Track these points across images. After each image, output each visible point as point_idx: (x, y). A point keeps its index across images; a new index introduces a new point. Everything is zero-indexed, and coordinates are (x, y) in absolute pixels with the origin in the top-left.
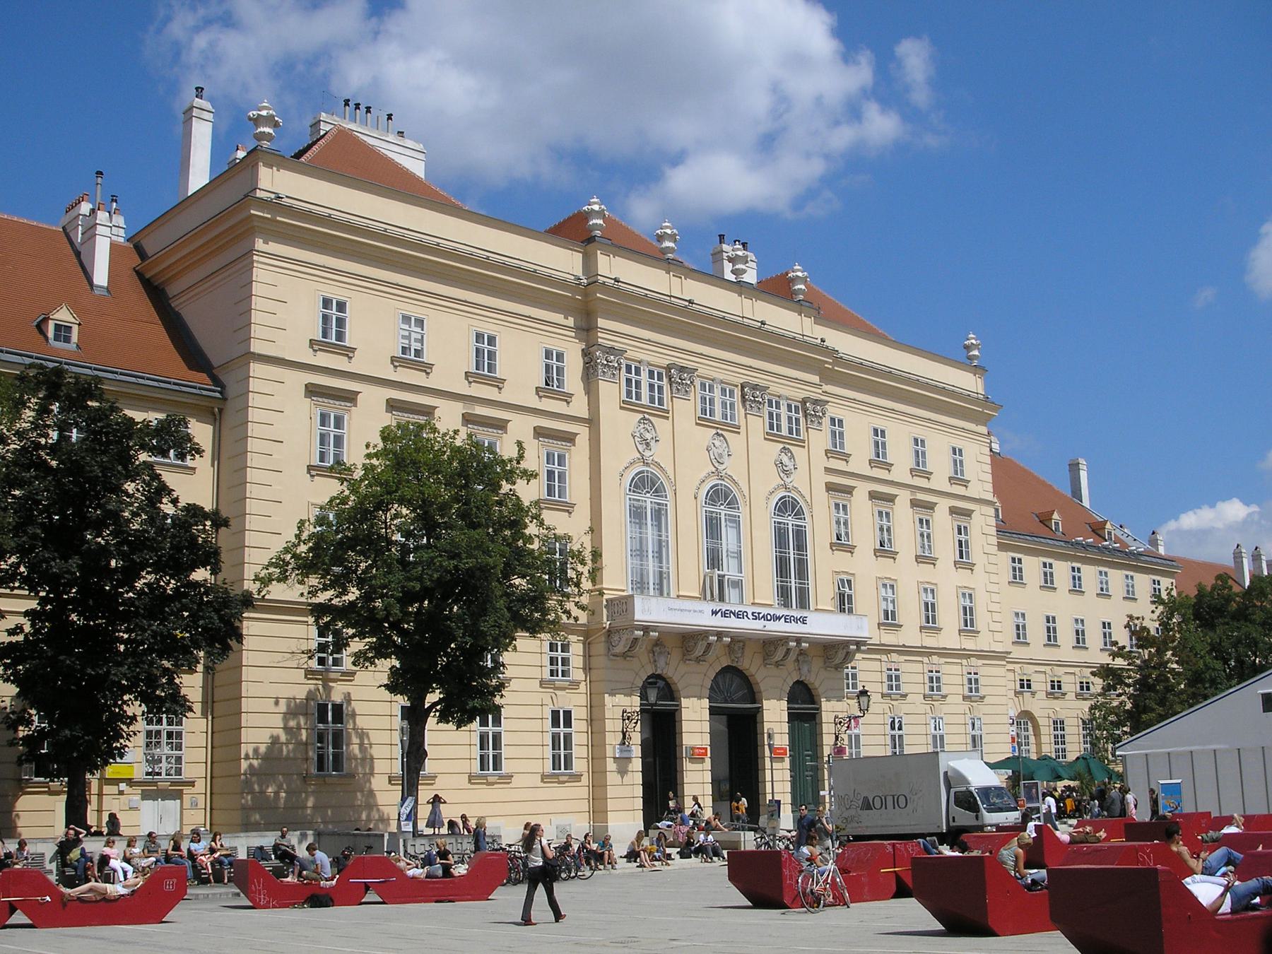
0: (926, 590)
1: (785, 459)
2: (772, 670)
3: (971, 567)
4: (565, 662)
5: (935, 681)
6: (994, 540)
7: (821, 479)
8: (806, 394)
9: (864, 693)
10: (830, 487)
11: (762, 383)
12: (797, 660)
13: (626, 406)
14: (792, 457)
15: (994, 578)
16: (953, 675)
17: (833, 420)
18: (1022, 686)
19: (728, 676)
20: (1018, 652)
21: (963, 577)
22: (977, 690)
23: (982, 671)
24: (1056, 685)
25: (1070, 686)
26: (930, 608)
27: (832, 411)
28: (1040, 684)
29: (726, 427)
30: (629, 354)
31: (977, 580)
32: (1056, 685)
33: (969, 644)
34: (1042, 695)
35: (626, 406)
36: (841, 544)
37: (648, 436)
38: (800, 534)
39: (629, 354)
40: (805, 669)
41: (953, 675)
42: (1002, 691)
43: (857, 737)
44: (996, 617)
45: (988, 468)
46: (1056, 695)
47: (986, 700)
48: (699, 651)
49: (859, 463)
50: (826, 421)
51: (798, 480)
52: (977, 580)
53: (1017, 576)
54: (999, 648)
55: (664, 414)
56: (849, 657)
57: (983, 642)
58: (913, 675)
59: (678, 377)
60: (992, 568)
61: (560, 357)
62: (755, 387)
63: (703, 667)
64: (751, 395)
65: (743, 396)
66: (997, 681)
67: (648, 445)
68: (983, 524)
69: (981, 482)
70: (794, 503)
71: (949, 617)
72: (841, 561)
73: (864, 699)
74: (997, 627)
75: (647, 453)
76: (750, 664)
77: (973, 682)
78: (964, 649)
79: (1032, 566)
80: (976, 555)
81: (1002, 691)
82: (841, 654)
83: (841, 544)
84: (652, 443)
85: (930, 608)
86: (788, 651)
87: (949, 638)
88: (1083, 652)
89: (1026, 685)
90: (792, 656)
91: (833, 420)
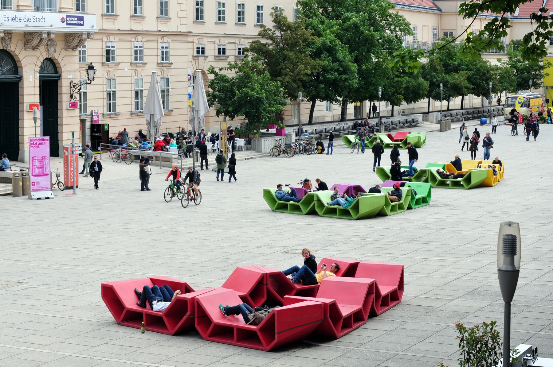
2: (30, 52)
12: (47, 45)
18: (198, 52)
23: (171, 46)
24: (222, 51)
28: (211, 51)
32: (222, 51)
33: (163, 27)
40: (52, 50)
42: (184, 59)
44: (183, 7)
46: (221, 58)
54: (183, 29)
57: (173, 26)
74: (182, 14)
77: (165, 55)
78: (160, 31)
81: (184, 59)
89: (201, 51)
90: (44, 42)
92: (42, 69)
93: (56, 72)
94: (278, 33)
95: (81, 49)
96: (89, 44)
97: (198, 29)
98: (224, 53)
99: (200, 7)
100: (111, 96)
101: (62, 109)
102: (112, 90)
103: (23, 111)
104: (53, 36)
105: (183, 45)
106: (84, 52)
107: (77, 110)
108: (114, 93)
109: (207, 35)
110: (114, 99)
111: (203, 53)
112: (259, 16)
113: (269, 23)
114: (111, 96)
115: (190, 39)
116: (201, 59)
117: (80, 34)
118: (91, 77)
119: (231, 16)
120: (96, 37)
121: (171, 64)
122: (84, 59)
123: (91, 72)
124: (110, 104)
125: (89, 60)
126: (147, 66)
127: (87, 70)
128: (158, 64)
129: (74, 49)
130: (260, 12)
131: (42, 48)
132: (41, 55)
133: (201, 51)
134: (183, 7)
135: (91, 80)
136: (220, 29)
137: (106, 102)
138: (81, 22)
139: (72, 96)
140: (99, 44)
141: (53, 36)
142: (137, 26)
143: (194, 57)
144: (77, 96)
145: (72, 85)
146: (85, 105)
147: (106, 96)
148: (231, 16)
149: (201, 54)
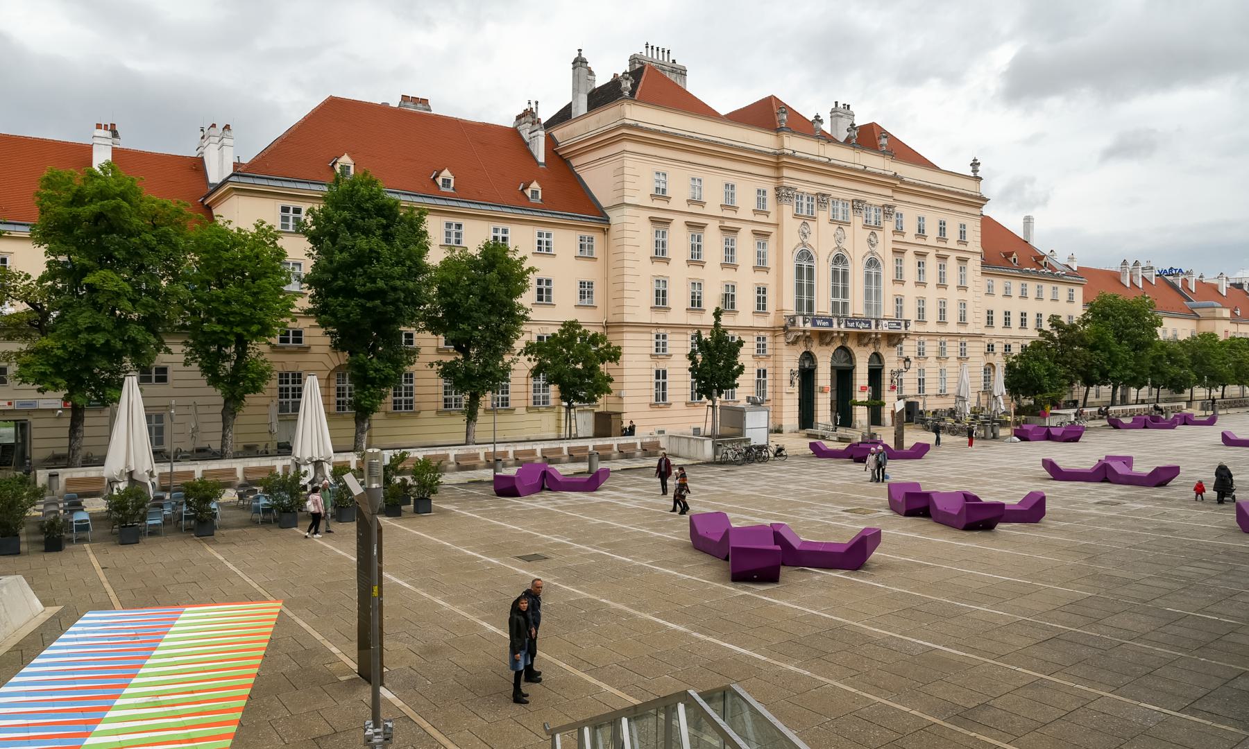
2: (862, 348)
3: (965, 288)
4: (764, 346)
5: (942, 350)
6: (980, 274)
7: (890, 246)
8: (882, 203)
9: (907, 360)
11: (863, 199)
13: (796, 216)
14: (876, 237)
15: (978, 294)
17: (897, 214)
18: (989, 350)
19: (839, 350)
20: (989, 332)
21: (961, 295)
22: (965, 354)
24: (1008, 347)
26: (942, 312)
27: (897, 210)
28: (999, 348)
29: (842, 224)
30: (799, 189)
31: (968, 296)
32: (1008, 347)
33: (963, 330)
34: (999, 355)
35: (796, 216)
36: (898, 280)
37: (806, 231)
38: (878, 276)
39: (799, 189)
41: (952, 348)
42: (978, 354)
43: (901, 379)
44: (978, 315)
45: (979, 234)
47: (969, 360)
48: (828, 339)
50: (894, 216)
51: (879, 249)
52: (968, 296)
53: (990, 293)
54: (978, 332)
55: (814, 219)
56: (900, 341)
58: (931, 348)
59: (822, 199)
60: (976, 289)
61: (764, 192)
62: (859, 201)
63: (829, 347)
64: (857, 206)
65: (853, 206)
66: (976, 350)
67: (806, 236)
68: (975, 263)
69: (974, 241)
70: (876, 261)
71: (952, 316)
72: (899, 290)
73: (907, 363)
74: (978, 320)
75: (805, 240)
76: (851, 345)
79: (999, 284)
80: (969, 283)
81: (978, 354)
82: (896, 341)
83: (898, 280)
84: (808, 235)
85: (942, 312)
86: (870, 339)
87: (952, 327)
88: (1025, 330)
89: (991, 348)
90: (873, 341)
91: (897, 214)
92: (870, 360)
93: (880, 363)
95: (899, 346)
96: (905, 342)
97: (989, 332)
99: (990, 315)
100: (921, 381)
102: (922, 377)
104: (879, 336)
106: (901, 349)
107: (896, 391)
108: (923, 379)
109: (996, 337)
110: (923, 384)
111: (992, 350)
112: (1039, 321)
113: (1046, 326)
114: (921, 381)
115: (983, 339)
117: (900, 334)
118: (907, 366)
119: (1015, 321)
120: (911, 337)
121: (968, 358)
122: (901, 353)
125: (905, 355)
126: (949, 360)
127: (905, 362)
128: (958, 358)
129: (894, 345)
130: (1024, 317)
131: (871, 345)
132: (870, 350)
133: (991, 348)
134: (978, 315)
135: (907, 369)
136: (1007, 332)
137: (917, 386)
140: (912, 343)
141: (879, 336)
142: (942, 329)
143: (985, 353)
144: (896, 380)
145: (892, 373)
146: (901, 388)
147: (917, 381)
148: (1015, 321)
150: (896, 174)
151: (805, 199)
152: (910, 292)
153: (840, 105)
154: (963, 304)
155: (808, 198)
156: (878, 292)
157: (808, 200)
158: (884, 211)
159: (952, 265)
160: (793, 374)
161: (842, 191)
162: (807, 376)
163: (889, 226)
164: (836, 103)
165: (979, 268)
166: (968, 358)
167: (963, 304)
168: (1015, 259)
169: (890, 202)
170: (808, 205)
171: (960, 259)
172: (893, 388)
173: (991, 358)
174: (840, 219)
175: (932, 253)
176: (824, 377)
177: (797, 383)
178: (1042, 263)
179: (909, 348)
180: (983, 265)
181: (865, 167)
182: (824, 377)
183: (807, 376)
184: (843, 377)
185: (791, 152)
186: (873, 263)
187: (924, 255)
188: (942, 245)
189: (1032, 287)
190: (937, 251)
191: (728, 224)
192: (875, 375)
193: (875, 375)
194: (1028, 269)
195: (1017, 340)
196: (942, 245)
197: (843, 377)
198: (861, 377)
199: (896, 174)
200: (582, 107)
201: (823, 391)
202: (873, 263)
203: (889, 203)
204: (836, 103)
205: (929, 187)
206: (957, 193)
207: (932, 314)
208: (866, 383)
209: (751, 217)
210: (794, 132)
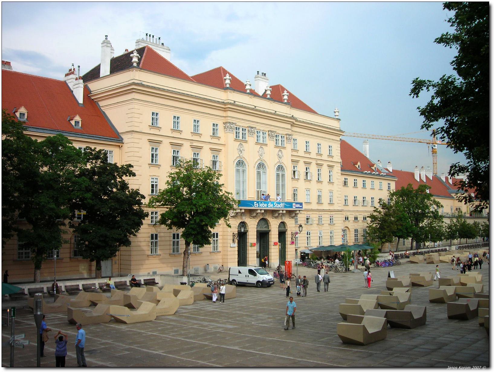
0: (319, 191)
1: (280, 154)
5: (320, 219)
7: (290, 158)
8: (287, 133)
9: (301, 226)
10: (292, 161)
13: (236, 140)
16: (326, 218)
17: (294, 139)
18: (346, 219)
20: (346, 208)
21: (330, 187)
24: (356, 218)
25: (360, 218)
28: (351, 218)
32: (356, 218)
33: (332, 208)
34: (351, 221)
35: (236, 140)
37: (241, 149)
38: (283, 175)
41: (326, 218)
45: (339, 152)
47: (336, 225)
49: (301, 153)
54: (340, 209)
55: (246, 142)
57: (336, 207)
64: (272, 134)
66: (339, 219)
68: (337, 168)
69: (337, 157)
70: (282, 167)
71: (325, 200)
80: (334, 179)
84: (243, 151)
87: (326, 206)
89: (347, 218)
90: (281, 215)
91: (294, 139)
92: (279, 226)
93: (285, 228)
94: (382, 210)
95: (296, 218)
97: (346, 208)
98: (357, 219)
101: (287, 244)
103: (271, 245)
105: (340, 216)
109: (349, 211)
110: (310, 239)
111: (348, 219)
113: (377, 205)
116: (347, 222)
122: (297, 222)
123: (301, 228)
124: (308, 242)
125: (299, 223)
128: (329, 224)
132: (279, 221)
133: (347, 218)
136: (356, 208)
138: (301, 206)
139: (292, 239)
149: (347, 220)
150: (293, 116)
151: (241, 130)
152: (301, 185)
153: (260, 73)
154: (331, 192)
155: (243, 129)
156: (283, 186)
157: (243, 130)
158: (287, 137)
159: (325, 170)
160: (234, 235)
161: (262, 124)
162: (242, 236)
163: (289, 146)
164: (258, 72)
165: (340, 171)
166: (334, 224)
167: (331, 192)
168: (359, 166)
169: (289, 132)
170: (243, 133)
171: (329, 166)
172: (293, 243)
173: (347, 224)
174: (261, 142)
175: (314, 162)
176: (252, 237)
177: (237, 241)
178: (373, 168)
179: (301, 218)
180: (342, 170)
181: (276, 112)
182: (252, 237)
183: (242, 236)
184: (263, 236)
185: (233, 102)
186: (280, 168)
187: (310, 163)
188: (319, 157)
189: (368, 181)
190: (316, 161)
191: (195, 144)
192: (282, 234)
193: (282, 234)
194: (366, 172)
195: (361, 213)
196: (319, 157)
197: (263, 236)
198: (274, 237)
199: (293, 116)
200: (105, 70)
201: (253, 245)
202: (280, 168)
203: (289, 133)
204: (258, 72)
205: (311, 124)
206: (327, 128)
207: (314, 200)
208: (277, 240)
209: (209, 139)
210: (234, 90)
